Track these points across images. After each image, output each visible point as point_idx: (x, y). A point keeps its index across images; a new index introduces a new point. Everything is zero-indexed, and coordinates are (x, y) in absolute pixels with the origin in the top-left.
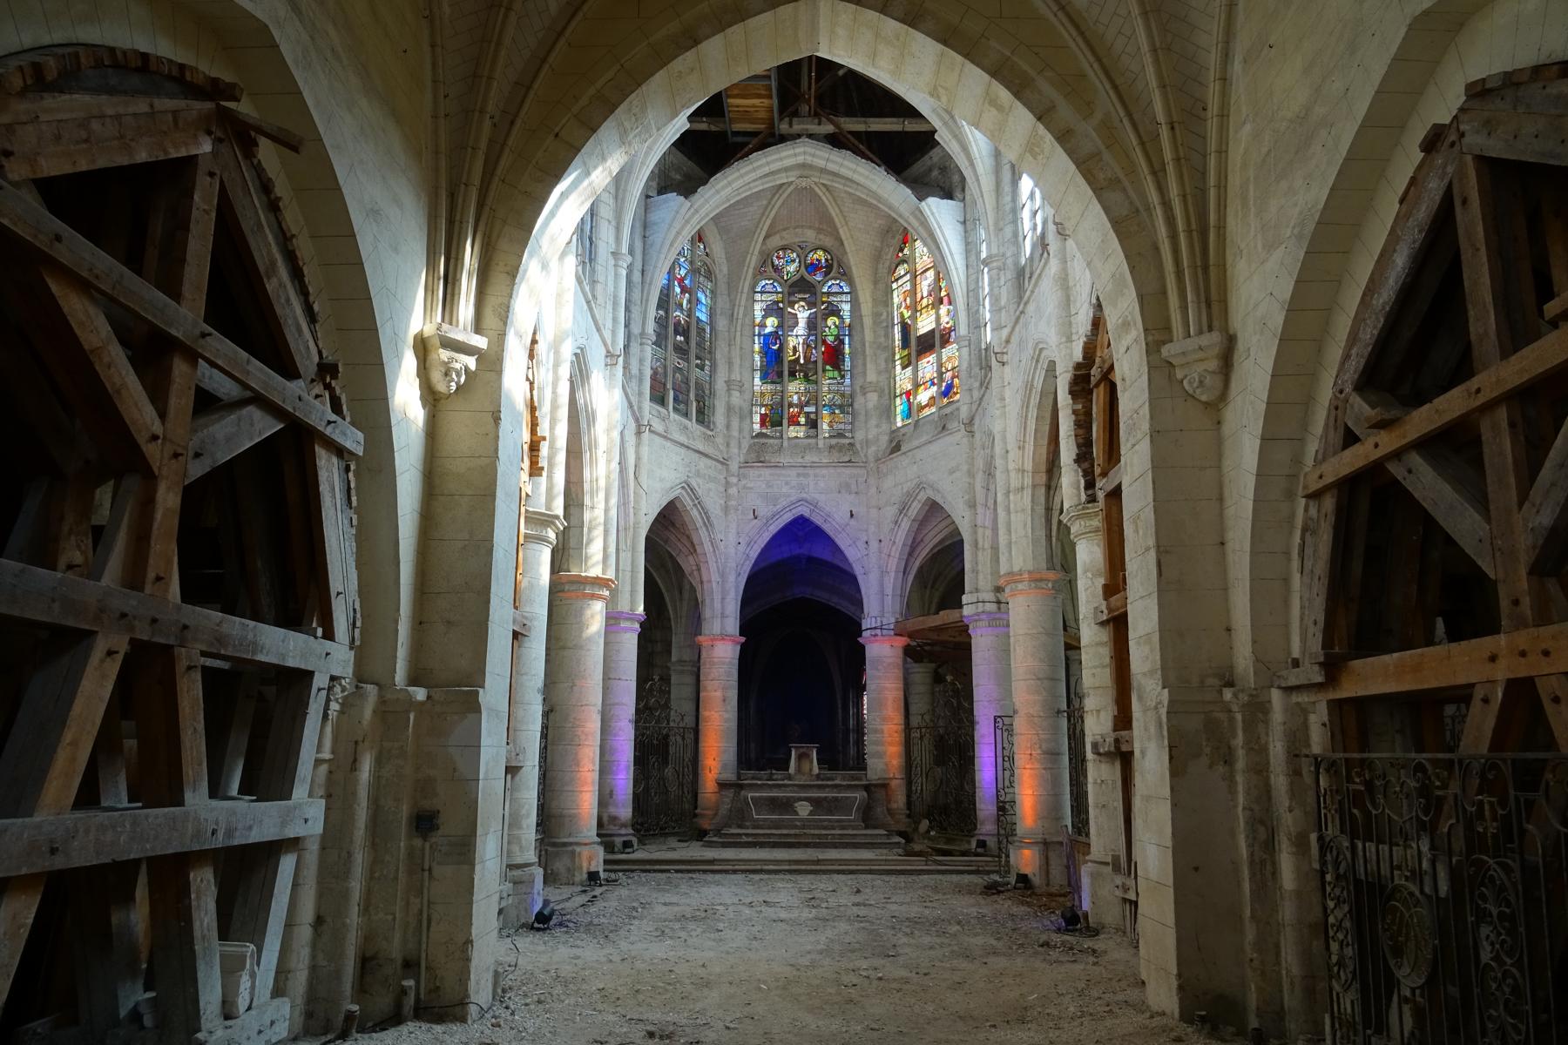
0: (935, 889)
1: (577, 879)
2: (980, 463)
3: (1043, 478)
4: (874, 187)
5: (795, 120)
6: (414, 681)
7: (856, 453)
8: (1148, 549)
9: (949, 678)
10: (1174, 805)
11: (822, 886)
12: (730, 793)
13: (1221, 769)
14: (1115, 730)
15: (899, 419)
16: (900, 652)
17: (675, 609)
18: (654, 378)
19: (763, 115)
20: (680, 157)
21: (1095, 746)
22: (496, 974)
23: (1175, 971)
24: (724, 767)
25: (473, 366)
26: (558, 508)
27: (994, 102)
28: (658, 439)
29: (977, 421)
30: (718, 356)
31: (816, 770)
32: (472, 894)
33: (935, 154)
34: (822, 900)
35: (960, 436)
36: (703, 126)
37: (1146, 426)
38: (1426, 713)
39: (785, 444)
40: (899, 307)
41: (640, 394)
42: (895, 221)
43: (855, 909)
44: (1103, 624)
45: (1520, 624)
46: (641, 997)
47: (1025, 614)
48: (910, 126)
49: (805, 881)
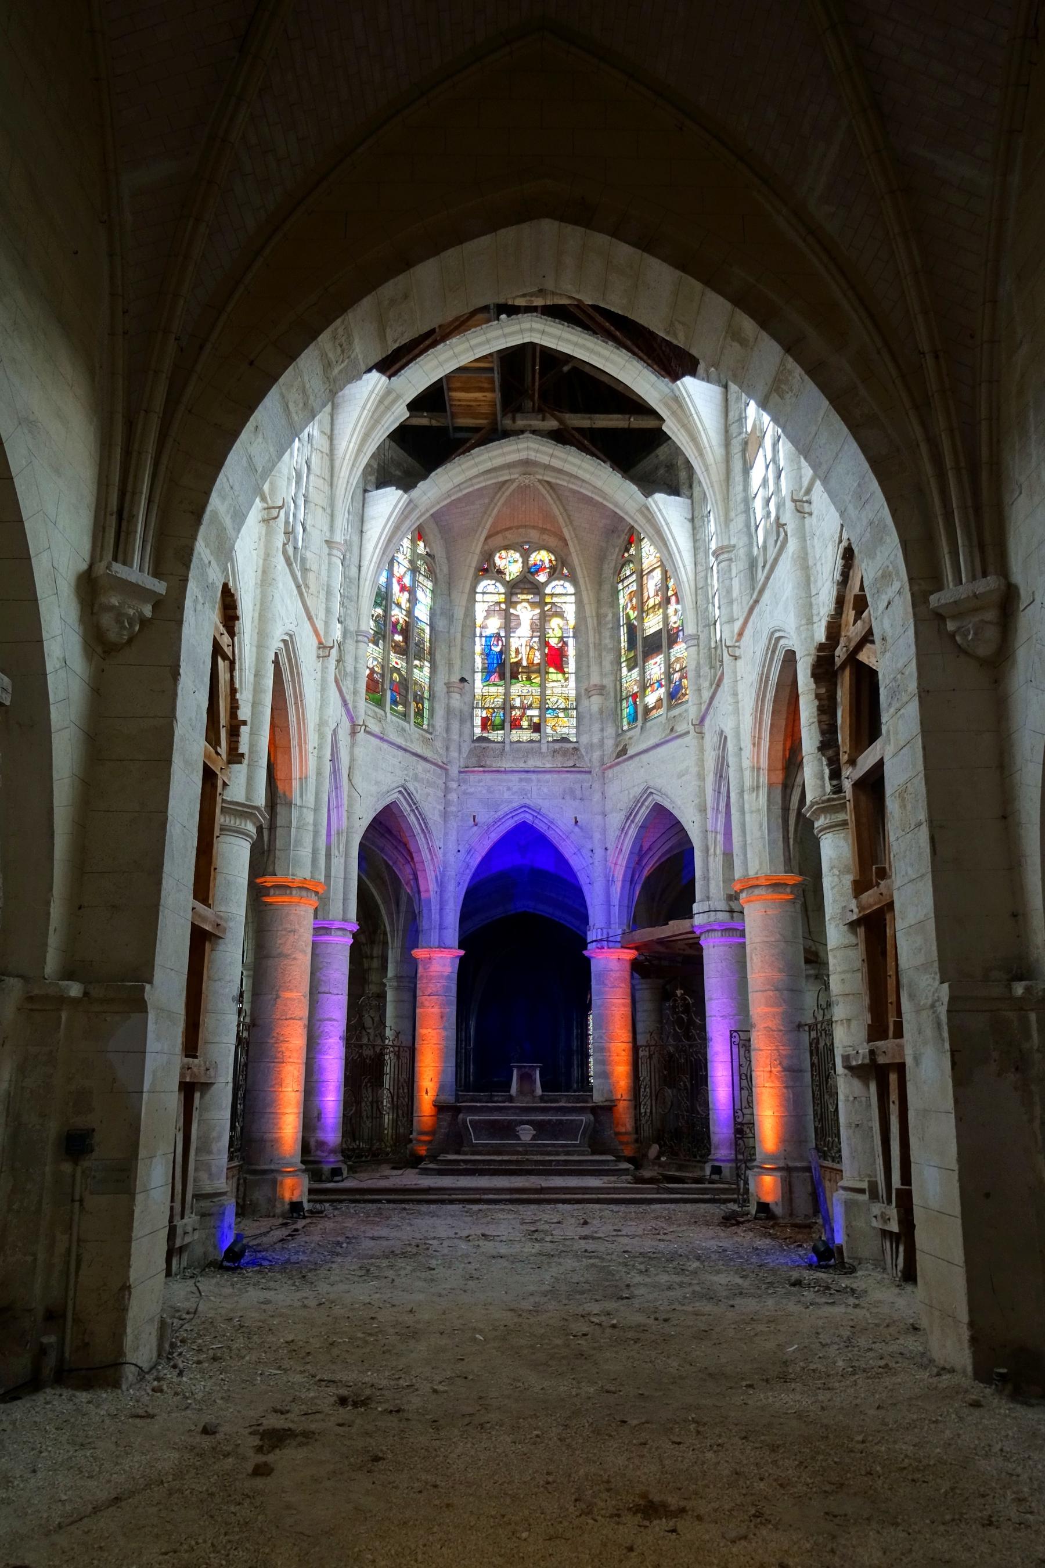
0: (669, 1219)
1: (278, 1211)
2: (710, 765)
3: (779, 777)
4: (599, 484)
5: (518, 416)
6: (69, 974)
7: (580, 757)
8: (920, 824)
9: (679, 992)
10: (959, 1120)
11: (546, 1217)
12: (447, 1117)
14: (869, 1041)
15: (625, 722)
16: (627, 966)
17: (392, 924)
18: (370, 677)
19: (485, 409)
20: (397, 453)
21: (846, 1058)
22: (163, 1324)
23: (965, 1318)
24: (441, 1089)
25: (147, 611)
26: (260, 799)
27: (735, 335)
28: (373, 739)
29: (707, 722)
30: (438, 657)
31: (539, 1091)
32: (130, 1228)
33: (662, 452)
34: (545, 1232)
35: (690, 740)
36: (423, 421)
37: (913, 686)
39: (507, 748)
40: (625, 608)
41: (355, 693)
42: (622, 519)
43: (582, 1242)
44: (853, 925)
46: (335, 1351)
47: (759, 919)
48: (637, 422)
49: (529, 1211)
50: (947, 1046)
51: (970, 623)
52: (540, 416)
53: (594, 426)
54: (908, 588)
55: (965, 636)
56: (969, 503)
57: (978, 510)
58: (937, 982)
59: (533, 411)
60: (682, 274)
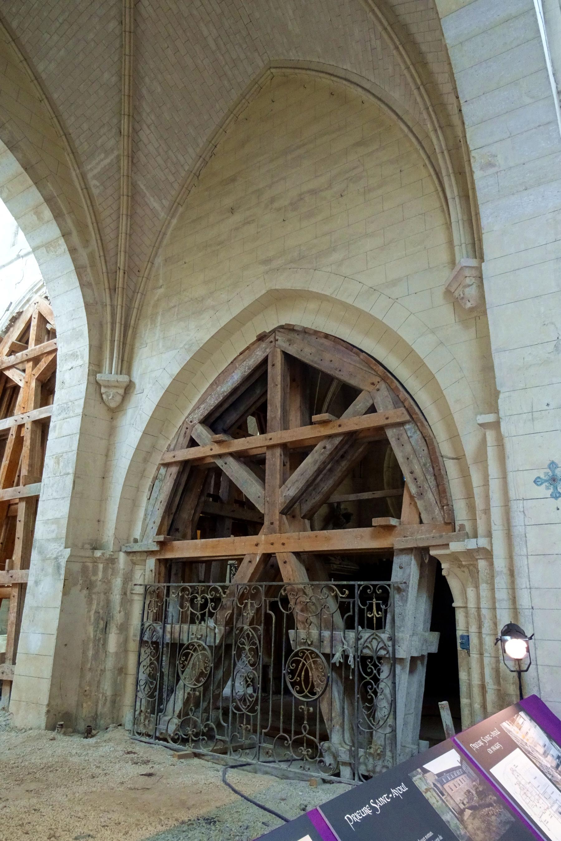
8: (68, 474)
10: (62, 611)
13: (85, 592)
23: (46, 702)
27: (38, 214)
37: (80, 410)
38: (186, 568)
45: (272, 531)
50: (62, 577)
51: (112, 392)
54: (87, 366)
55: (108, 396)
56: (122, 340)
57: (124, 344)
58: (62, 548)
60: (24, 171)
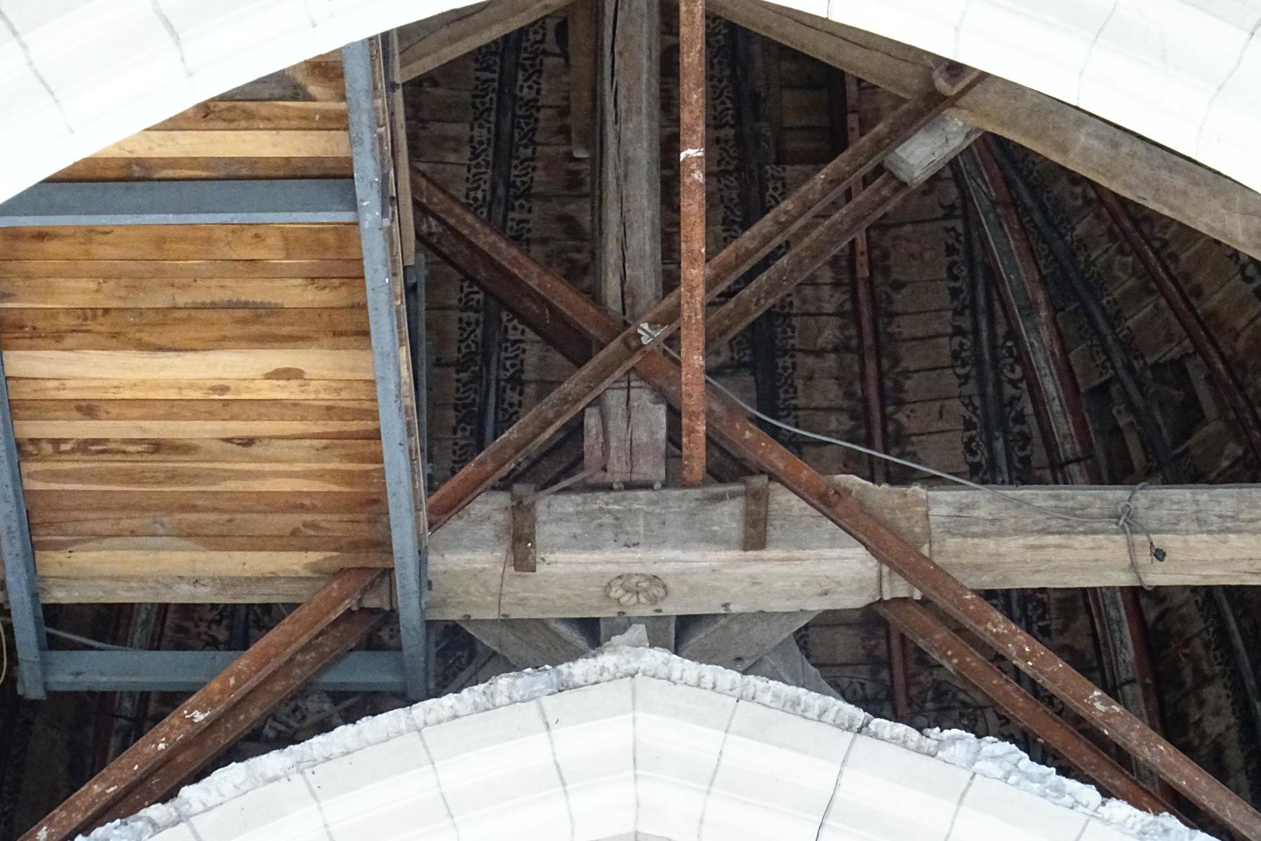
5: (556, 512)
19: (294, 470)
52: (729, 514)
53: (1157, 576)
59: (674, 479)
